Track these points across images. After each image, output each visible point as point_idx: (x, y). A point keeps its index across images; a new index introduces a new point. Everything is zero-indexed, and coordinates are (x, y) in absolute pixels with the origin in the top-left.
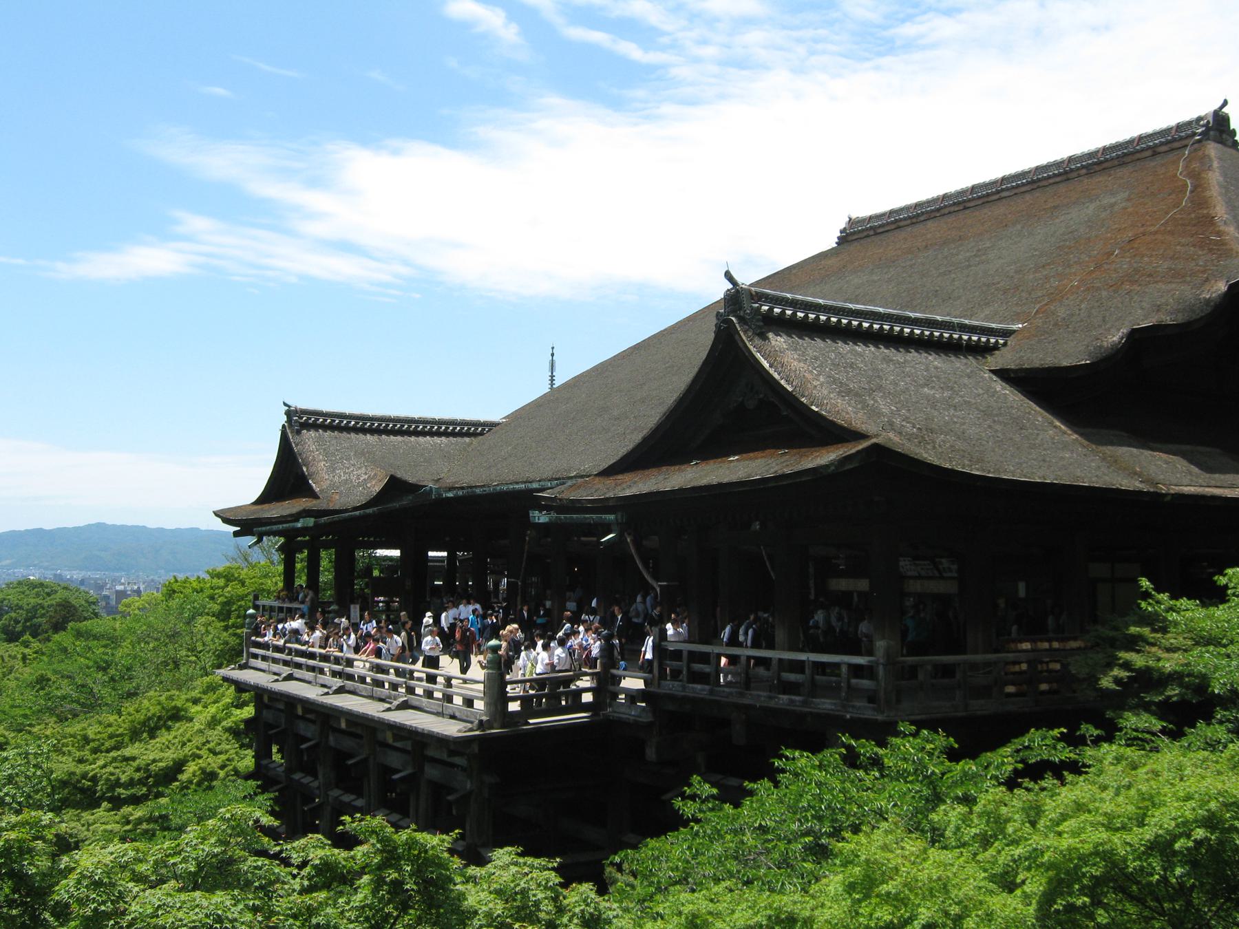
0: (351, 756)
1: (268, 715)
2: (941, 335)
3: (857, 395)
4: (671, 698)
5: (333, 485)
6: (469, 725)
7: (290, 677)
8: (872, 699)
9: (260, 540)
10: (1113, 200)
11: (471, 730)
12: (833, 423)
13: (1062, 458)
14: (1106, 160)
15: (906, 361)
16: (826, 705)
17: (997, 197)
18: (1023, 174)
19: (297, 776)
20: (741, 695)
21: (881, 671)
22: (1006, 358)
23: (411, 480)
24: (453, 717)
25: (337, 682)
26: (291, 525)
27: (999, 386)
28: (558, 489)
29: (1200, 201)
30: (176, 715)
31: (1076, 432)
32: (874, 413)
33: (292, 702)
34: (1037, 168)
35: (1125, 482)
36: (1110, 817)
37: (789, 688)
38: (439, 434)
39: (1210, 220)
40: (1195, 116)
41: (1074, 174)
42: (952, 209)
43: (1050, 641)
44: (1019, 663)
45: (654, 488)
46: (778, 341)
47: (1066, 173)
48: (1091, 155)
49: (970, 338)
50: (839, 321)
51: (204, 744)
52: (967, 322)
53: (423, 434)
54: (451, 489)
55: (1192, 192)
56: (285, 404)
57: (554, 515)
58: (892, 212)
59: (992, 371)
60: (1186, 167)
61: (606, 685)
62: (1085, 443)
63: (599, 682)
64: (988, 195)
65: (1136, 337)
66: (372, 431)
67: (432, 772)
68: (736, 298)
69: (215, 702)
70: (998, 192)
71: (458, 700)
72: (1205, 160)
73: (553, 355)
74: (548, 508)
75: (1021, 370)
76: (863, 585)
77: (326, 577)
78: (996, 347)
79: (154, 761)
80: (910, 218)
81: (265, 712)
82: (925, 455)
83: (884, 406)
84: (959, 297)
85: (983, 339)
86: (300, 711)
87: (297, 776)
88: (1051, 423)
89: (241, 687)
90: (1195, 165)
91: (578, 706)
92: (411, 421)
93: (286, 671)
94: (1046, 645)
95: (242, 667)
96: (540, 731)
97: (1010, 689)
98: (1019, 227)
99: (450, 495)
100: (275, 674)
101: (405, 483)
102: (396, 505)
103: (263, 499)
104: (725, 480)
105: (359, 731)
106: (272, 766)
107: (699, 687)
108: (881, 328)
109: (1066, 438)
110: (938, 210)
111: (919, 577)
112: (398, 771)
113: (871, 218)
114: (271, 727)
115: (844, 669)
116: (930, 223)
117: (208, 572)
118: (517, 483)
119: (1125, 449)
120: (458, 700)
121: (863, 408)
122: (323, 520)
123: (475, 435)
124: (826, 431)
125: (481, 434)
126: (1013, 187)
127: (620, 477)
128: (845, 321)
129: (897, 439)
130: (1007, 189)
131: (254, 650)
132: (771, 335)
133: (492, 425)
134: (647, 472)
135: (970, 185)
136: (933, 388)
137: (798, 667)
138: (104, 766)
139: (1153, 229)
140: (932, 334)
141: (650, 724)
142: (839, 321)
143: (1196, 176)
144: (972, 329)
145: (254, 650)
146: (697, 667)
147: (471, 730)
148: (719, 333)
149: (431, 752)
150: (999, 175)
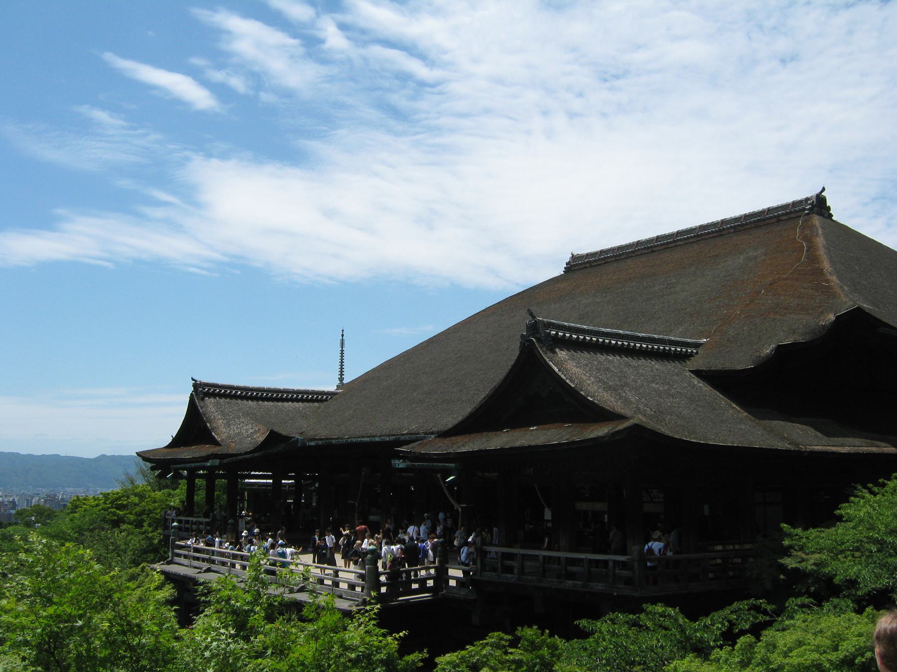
3: (615, 390)
5: (229, 437)
7: (208, 570)
8: (629, 582)
10: (755, 254)
13: (741, 429)
14: (747, 224)
15: (639, 366)
16: (598, 587)
17: (673, 245)
18: (690, 231)
22: (698, 362)
23: (284, 433)
24: (340, 597)
27: (696, 381)
28: (411, 445)
29: (813, 259)
31: (746, 411)
32: (627, 402)
36: (818, 647)
37: (571, 576)
39: (820, 272)
40: (804, 197)
41: (725, 232)
42: (644, 252)
43: (733, 544)
44: (715, 559)
45: (482, 447)
46: (562, 354)
47: (720, 230)
48: (736, 219)
54: (312, 440)
55: (807, 251)
56: (193, 379)
58: (602, 252)
59: (690, 371)
60: (802, 232)
61: (441, 577)
62: (753, 418)
64: (668, 243)
65: (780, 349)
69: (138, 587)
70: (674, 241)
71: (343, 586)
72: (813, 226)
75: (710, 371)
76: (599, 506)
78: (691, 355)
83: (632, 397)
84: (660, 318)
88: (730, 405)
89: (170, 578)
90: (807, 232)
91: (423, 588)
92: (278, 391)
93: (205, 565)
94: (731, 547)
95: (169, 563)
97: (711, 575)
98: (693, 269)
99: (313, 444)
104: (533, 444)
107: (509, 576)
109: (740, 416)
110: (633, 252)
113: (587, 255)
115: (611, 564)
116: (629, 261)
117: (101, 493)
118: (363, 437)
119: (776, 422)
120: (343, 586)
122: (225, 461)
123: (321, 401)
124: (600, 414)
125: (326, 400)
126: (685, 239)
127: (453, 438)
129: (644, 419)
130: (681, 240)
131: (177, 551)
132: (557, 350)
134: (473, 436)
135: (655, 235)
136: (657, 383)
139: (785, 276)
142: (598, 340)
143: (809, 240)
144: (676, 343)
145: (177, 551)
146: (508, 562)
148: (523, 348)
150: (675, 230)
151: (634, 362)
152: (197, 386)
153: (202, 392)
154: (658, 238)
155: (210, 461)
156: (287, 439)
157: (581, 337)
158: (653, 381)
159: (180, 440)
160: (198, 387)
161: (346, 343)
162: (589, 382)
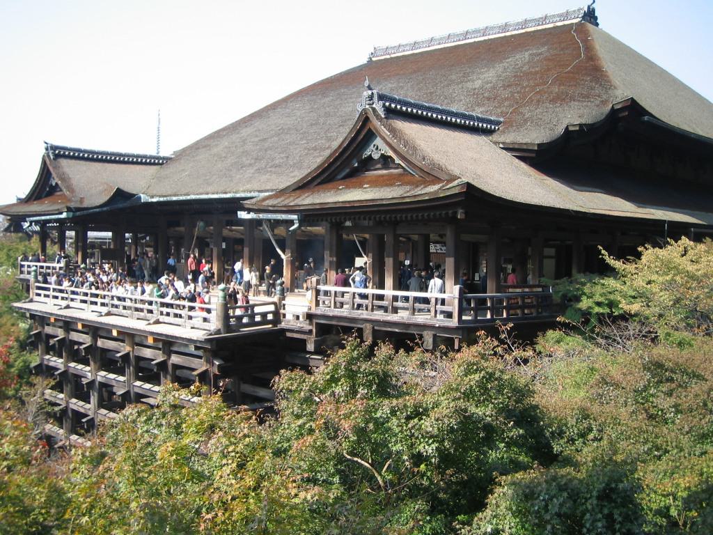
7: (68, 307)
26: (56, 217)
28: (254, 200)
45: (322, 201)
56: (46, 143)
67: (175, 359)
74: (249, 210)
81: (46, 327)
87: (72, 365)
93: (64, 303)
99: (155, 200)
102: (120, 206)
112: (153, 360)
122: (78, 213)
125: (162, 164)
141: (311, 331)
147: (211, 335)
149: (175, 349)
161: (161, 120)
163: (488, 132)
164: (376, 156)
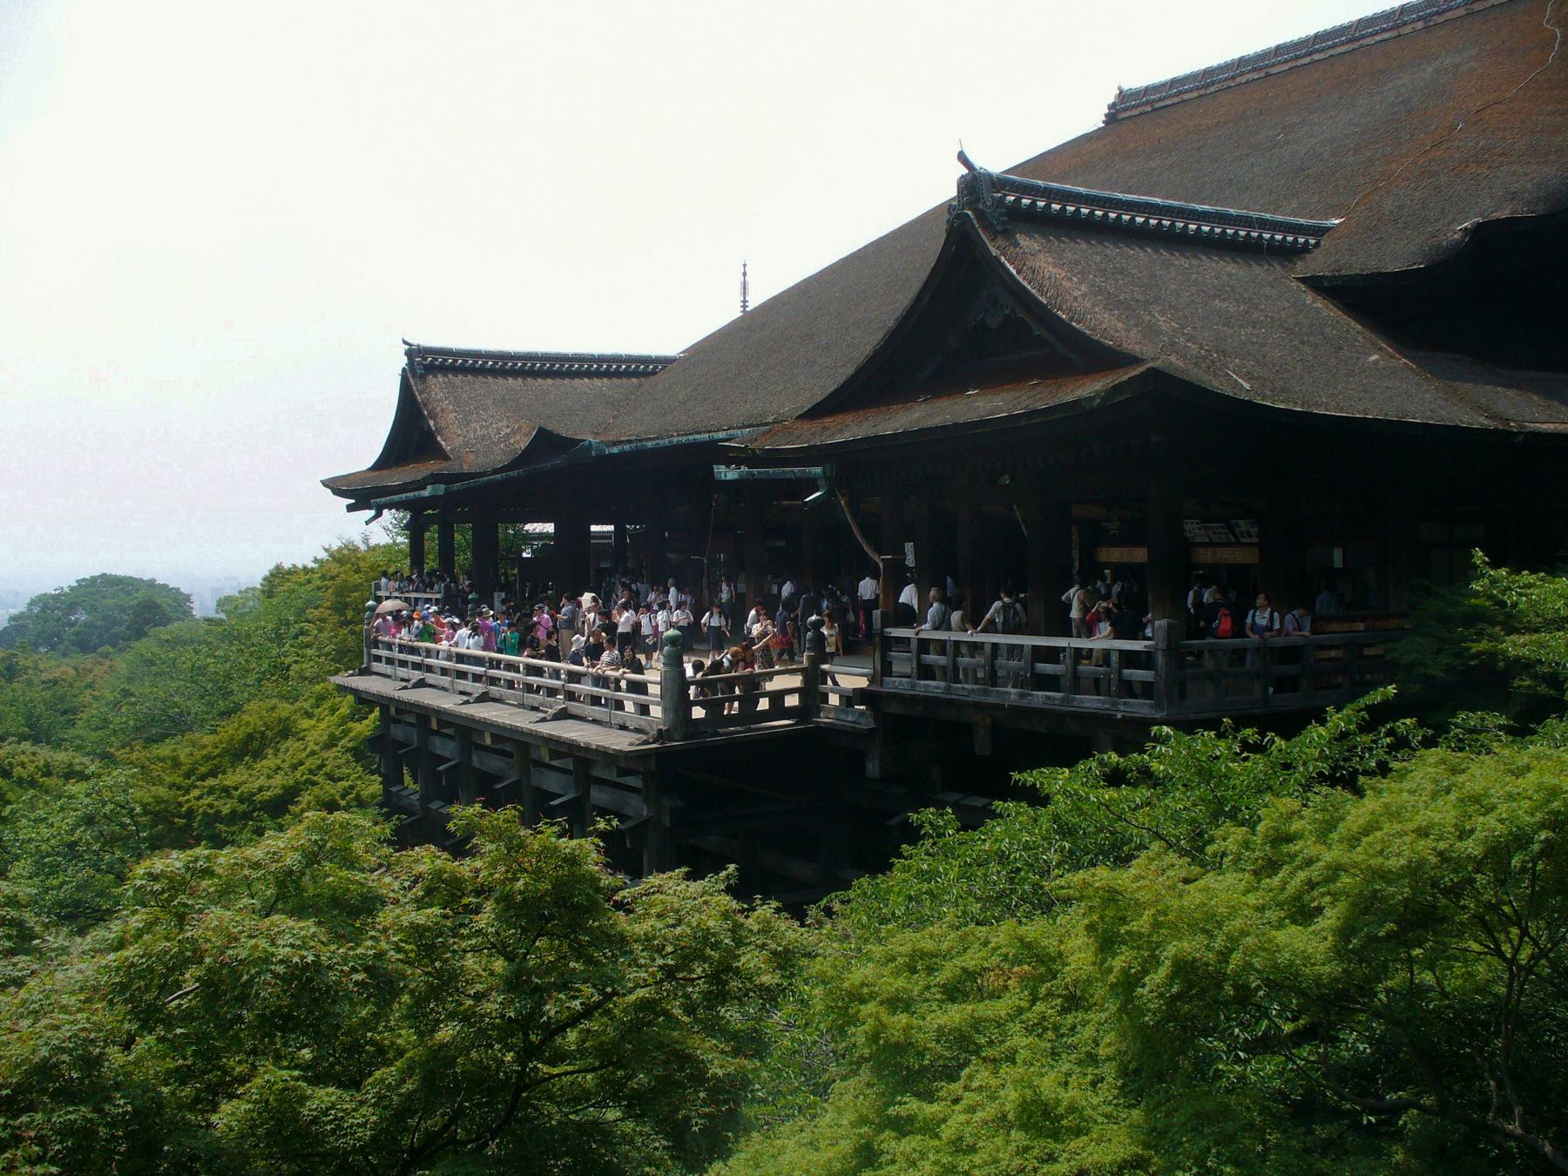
0: (498, 779)
1: (397, 732)
2: (1236, 233)
4: (894, 697)
6: (644, 737)
7: (421, 684)
9: (379, 515)
11: (646, 742)
12: (1098, 342)
16: (1089, 702)
19: (434, 806)
20: (986, 693)
21: (1160, 659)
24: (623, 727)
25: (478, 688)
27: (1309, 297)
30: (286, 731)
32: (1151, 331)
33: (423, 714)
34: (1360, 21)
35: (1466, 418)
38: (599, 374)
42: (1250, 76)
45: (871, 432)
49: (1272, 237)
50: (1105, 215)
51: (320, 767)
52: (1268, 216)
53: (579, 374)
54: (615, 443)
56: (405, 343)
57: (744, 469)
59: (1302, 280)
63: (806, 680)
64: (1297, 58)
66: (514, 373)
68: (974, 185)
73: (745, 274)
74: (738, 462)
77: (463, 559)
78: (1305, 249)
79: (261, 789)
80: (1198, 89)
82: (1216, 384)
83: (1163, 322)
85: (1290, 239)
86: (434, 726)
87: (434, 806)
93: (416, 675)
96: (733, 745)
99: (615, 450)
100: (403, 680)
101: (558, 436)
103: (380, 465)
105: (508, 749)
106: (404, 793)
108: (1160, 224)
109: (1394, 363)
111: (1212, 544)
112: (560, 796)
114: (401, 745)
115: (1114, 657)
121: (1136, 325)
122: (456, 486)
123: (645, 374)
125: (653, 373)
128: (1112, 215)
131: (374, 651)
133: (666, 362)
134: (861, 413)
137: (1052, 655)
138: (198, 798)
140: (1224, 231)
142: (1105, 215)
145: (374, 651)
147: (646, 742)
148: (950, 231)
149: (596, 772)
150: (1312, 32)
151: (1180, 261)
152: (414, 353)
153: (425, 365)
154: (1279, 50)
155: (429, 488)
156: (571, 443)
157: (1071, 209)
158: (1214, 297)
159: (394, 454)
160: (414, 353)
162: (1076, 293)
163: (1287, 254)
164: (994, 323)
